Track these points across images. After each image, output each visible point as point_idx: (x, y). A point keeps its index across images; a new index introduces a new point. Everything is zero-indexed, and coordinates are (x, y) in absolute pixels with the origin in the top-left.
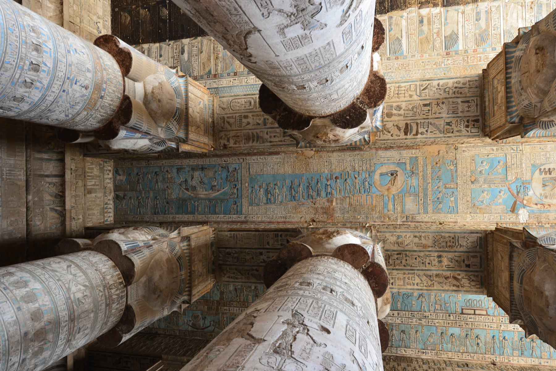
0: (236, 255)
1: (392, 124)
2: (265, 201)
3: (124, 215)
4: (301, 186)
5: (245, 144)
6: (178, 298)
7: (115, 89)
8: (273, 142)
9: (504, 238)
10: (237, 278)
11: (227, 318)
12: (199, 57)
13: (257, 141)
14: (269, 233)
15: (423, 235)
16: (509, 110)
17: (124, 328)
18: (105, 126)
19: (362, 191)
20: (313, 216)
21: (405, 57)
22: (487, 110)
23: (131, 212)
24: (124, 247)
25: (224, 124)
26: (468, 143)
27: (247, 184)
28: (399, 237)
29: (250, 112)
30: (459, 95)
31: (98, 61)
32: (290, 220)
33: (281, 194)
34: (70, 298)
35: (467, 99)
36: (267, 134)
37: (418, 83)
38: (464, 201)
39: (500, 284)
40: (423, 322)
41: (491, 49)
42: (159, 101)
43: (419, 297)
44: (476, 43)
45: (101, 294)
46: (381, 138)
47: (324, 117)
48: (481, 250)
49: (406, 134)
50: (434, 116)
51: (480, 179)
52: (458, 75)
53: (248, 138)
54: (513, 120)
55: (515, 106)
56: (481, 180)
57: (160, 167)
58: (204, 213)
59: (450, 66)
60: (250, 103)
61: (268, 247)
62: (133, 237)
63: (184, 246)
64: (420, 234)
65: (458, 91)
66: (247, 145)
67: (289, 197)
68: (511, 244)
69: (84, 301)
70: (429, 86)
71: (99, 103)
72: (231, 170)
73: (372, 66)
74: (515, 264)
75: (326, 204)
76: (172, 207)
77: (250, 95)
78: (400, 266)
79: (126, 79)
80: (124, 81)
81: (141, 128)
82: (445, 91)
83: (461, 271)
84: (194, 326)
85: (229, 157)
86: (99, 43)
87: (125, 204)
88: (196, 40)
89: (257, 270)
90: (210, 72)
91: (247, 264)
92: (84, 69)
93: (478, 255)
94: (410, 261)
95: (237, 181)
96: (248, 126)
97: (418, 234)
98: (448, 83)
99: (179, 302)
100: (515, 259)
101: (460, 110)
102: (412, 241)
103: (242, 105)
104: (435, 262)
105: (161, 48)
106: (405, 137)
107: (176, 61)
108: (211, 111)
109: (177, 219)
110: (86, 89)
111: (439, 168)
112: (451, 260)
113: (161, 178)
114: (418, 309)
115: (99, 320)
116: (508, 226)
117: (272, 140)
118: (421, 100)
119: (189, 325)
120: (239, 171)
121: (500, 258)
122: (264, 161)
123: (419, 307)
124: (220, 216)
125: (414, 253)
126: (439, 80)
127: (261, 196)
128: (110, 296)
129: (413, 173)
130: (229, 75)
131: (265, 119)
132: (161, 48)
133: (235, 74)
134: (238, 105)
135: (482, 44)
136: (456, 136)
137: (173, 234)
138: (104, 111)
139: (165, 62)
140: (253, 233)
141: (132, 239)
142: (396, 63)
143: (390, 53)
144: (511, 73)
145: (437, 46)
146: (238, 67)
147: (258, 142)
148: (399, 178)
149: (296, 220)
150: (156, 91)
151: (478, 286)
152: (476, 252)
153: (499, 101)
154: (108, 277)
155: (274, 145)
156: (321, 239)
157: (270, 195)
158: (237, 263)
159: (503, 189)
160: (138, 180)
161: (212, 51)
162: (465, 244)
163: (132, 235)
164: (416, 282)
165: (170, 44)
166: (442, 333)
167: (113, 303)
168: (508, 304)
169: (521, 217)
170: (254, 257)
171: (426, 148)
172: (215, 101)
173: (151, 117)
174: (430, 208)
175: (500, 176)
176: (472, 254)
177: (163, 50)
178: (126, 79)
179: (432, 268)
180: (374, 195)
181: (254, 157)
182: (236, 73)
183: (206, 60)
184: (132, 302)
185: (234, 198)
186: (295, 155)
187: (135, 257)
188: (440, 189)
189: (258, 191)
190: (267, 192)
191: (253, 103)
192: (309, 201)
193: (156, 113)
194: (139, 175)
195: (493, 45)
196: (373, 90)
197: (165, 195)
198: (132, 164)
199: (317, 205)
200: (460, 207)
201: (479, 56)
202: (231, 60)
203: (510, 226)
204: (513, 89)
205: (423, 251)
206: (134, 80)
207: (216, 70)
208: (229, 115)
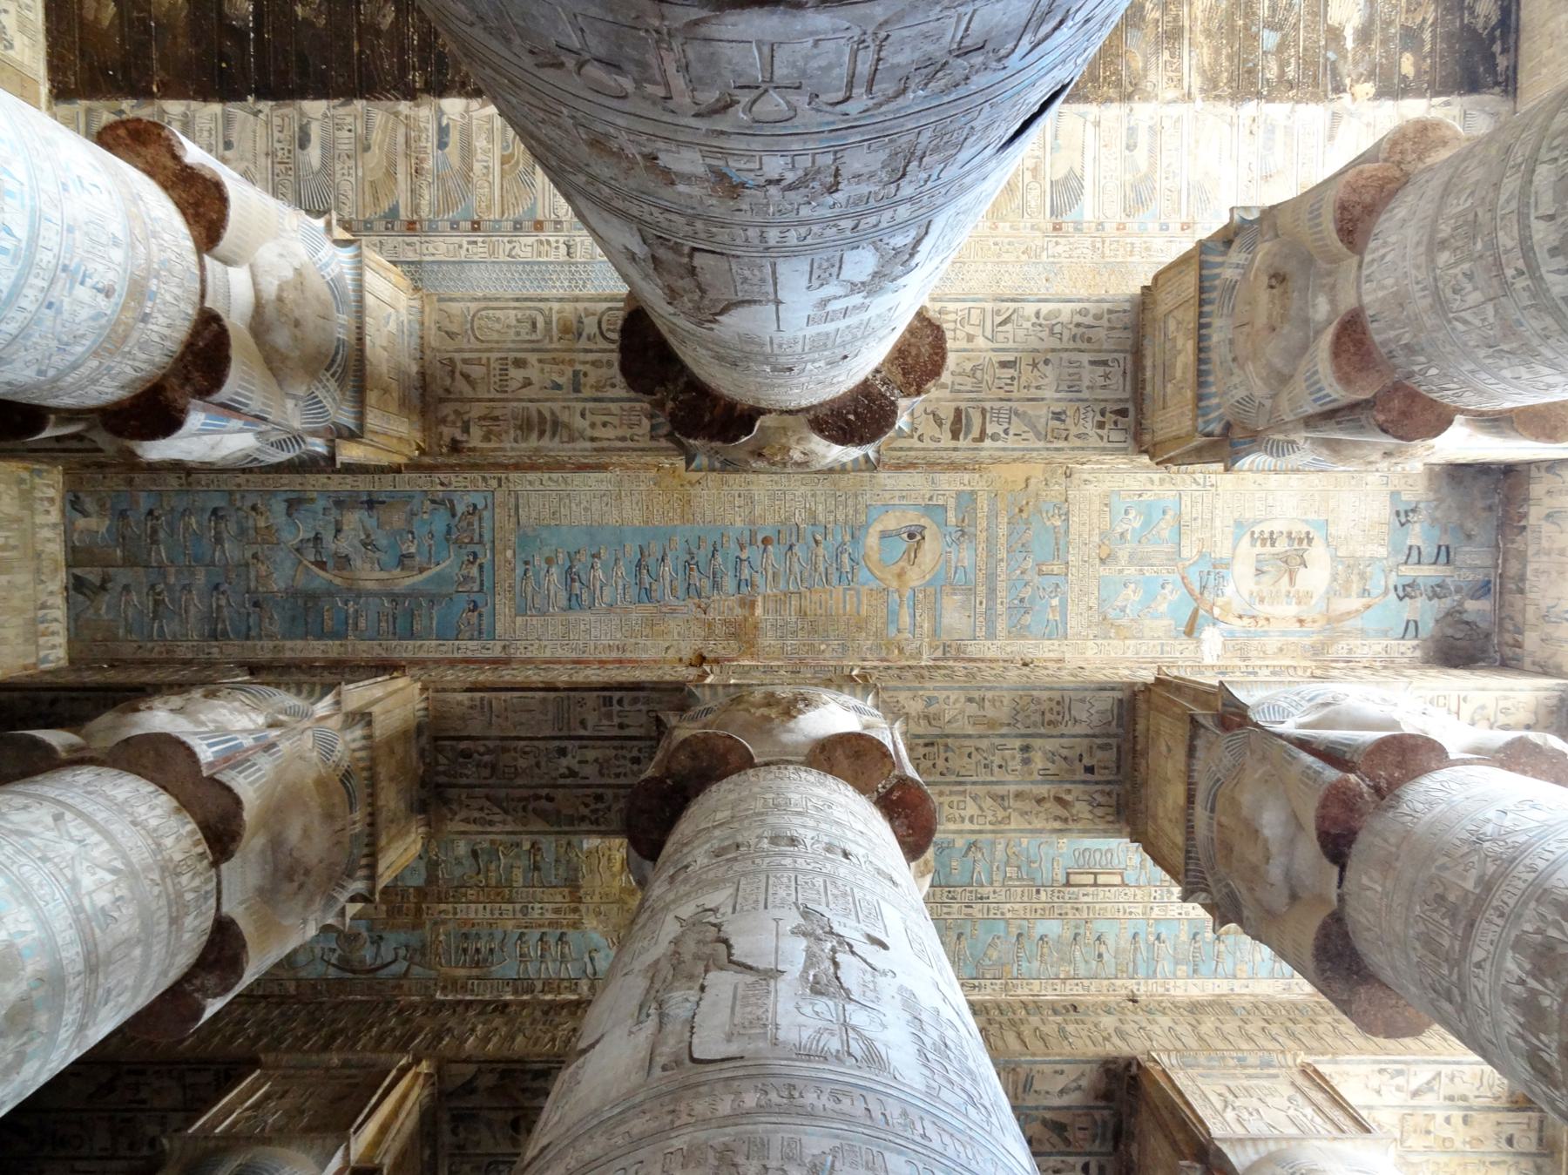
0: (486, 758)
2: (564, 603)
3: (105, 640)
4: (668, 560)
5: (516, 441)
6: (343, 887)
7: (178, 291)
8: (601, 439)
9: (1175, 703)
10: (491, 823)
11: (448, 934)
13: (554, 435)
14: (585, 694)
15: (989, 695)
16: (1203, 404)
17: (211, 981)
18: (137, 397)
19: (834, 578)
20: (699, 644)
22: (1149, 389)
23: (129, 631)
24: (206, 753)
25: (453, 379)
26: (1098, 462)
27: (509, 553)
28: (930, 701)
29: (533, 350)
30: (1085, 346)
31: (134, 210)
32: (634, 656)
33: (612, 581)
35: (1103, 357)
36: (583, 415)
37: (988, 306)
38: (1083, 607)
39: (1161, 813)
40: (976, 911)
41: (1157, 226)
42: (297, 324)
43: (969, 849)
45: (156, 890)
47: (790, 412)
48: (1121, 731)
49: (955, 436)
50: (1024, 393)
51: (1120, 554)
52: (1083, 293)
53: (527, 426)
54: (1209, 429)
55: (1215, 395)
56: (1123, 555)
57: (231, 493)
58: (377, 636)
60: (534, 325)
61: (582, 732)
62: (214, 721)
63: (354, 740)
64: (981, 693)
66: (524, 445)
67: (633, 591)
68: (1193, 721)
69: (116, 914)
70: (1014, 317)
71: (135, 335)
72: (460, 509)
74: (1198, 765)
75: (738, 611)
76: (271, 618)
77: (531, 300)
78: (930, 774)
79: (207, 259)
80: (202, 267)
81: (246, 405)
82: (1052, 333)
83: (1074, 782)
84: (344, 964)
85: (454, 472)
86: (111, 141)
87: (108, 607)
88: (348, 109)
89: (550, 799)
90: (394, 211)
91: (519, 781)
92: (104, 240)
93: (1113, 741)
94: (955, 763)
95: (481, 542)
96: (524, 390)
97: (976, 695)
98: (1059, 311)
99: (343, 898)
100: (1200, 754)
101: (1086, 383)
102: (962, 712)
104: (1016, 764)
105: (228, 121)
106: (953, 444)
107: (282, 167)
108: (415, 341)
109: (288, 654)
110: (107, 296)
111: (1027, 522)
112: (1051, 757)
113: (233, 528)
114: (967, 881)
115: (153, 963)
116: (1183, 674)
117: (596, 434)
119: (328, 963)
120: (486, 514)
121: (1164, 749)
122: (563, 487)
123: (968, 874)
125: (967, 742)
126: (1039, 301)
127: (552, 588)
128: (180, 895)
129: (963, 533)
130: (454, 226)
131: (576, 374)
132: (228, 121)
133: (476, 226)
134: (497, 326)
136: (1073, 449)
137: (320, 705)
138: (144, 357)
139: (243, 165)
140: (541, 694)
141: (212, 726)
144: (1209, 314)
147: (557, 439)
148: (927, 545)
149: (651, 654)
150: (290, 296)
151: (1110, 818)
152: (1108, 736)
153: (1179, 374)
154: (169, 842)
155: (603, 449)
156: (768, 719)
157: (577, 584)
158: (490, 781)
159: (1171, 577)
160: (154, 531)
161: (401, 147)
162: (1084, 716)
163: (211, 716)
164: (967, 813)
166: (1020, 935)
167: (187, 914)
168: (1178, 858)
169: (1205, 647)
170: (543, 764)
171: (996, 471)
172: (427, 309)
173: (271, 369)
174: (1001, 625)
175: (1166, 548)
176: (1099, 741)
177: (237, 126)
178: (207, 259)
179: (1009, 778)
180: (864, 590)
181: (531, 476)
182: (478, 223)
183: (380, 174)
184: (231, 908)
186: (654, 472)
187: (240, 778)
188: (1027, 577)
189: (543, 573)
190: (570, 576)
192: (689, 602)
193: (287, 358)
194: (157, 518)
196: (914, 352)
197: (248, 579)
198: (130, 482)
199: (710, 617)
200: (1072, 622)
201: (1129, 240)
202: (461, 182)
203: (1188, 675)
204: (1214, 356)
205: (987, 736)
206: (226, 262)
207: (416, 209)
208: (467, 355)
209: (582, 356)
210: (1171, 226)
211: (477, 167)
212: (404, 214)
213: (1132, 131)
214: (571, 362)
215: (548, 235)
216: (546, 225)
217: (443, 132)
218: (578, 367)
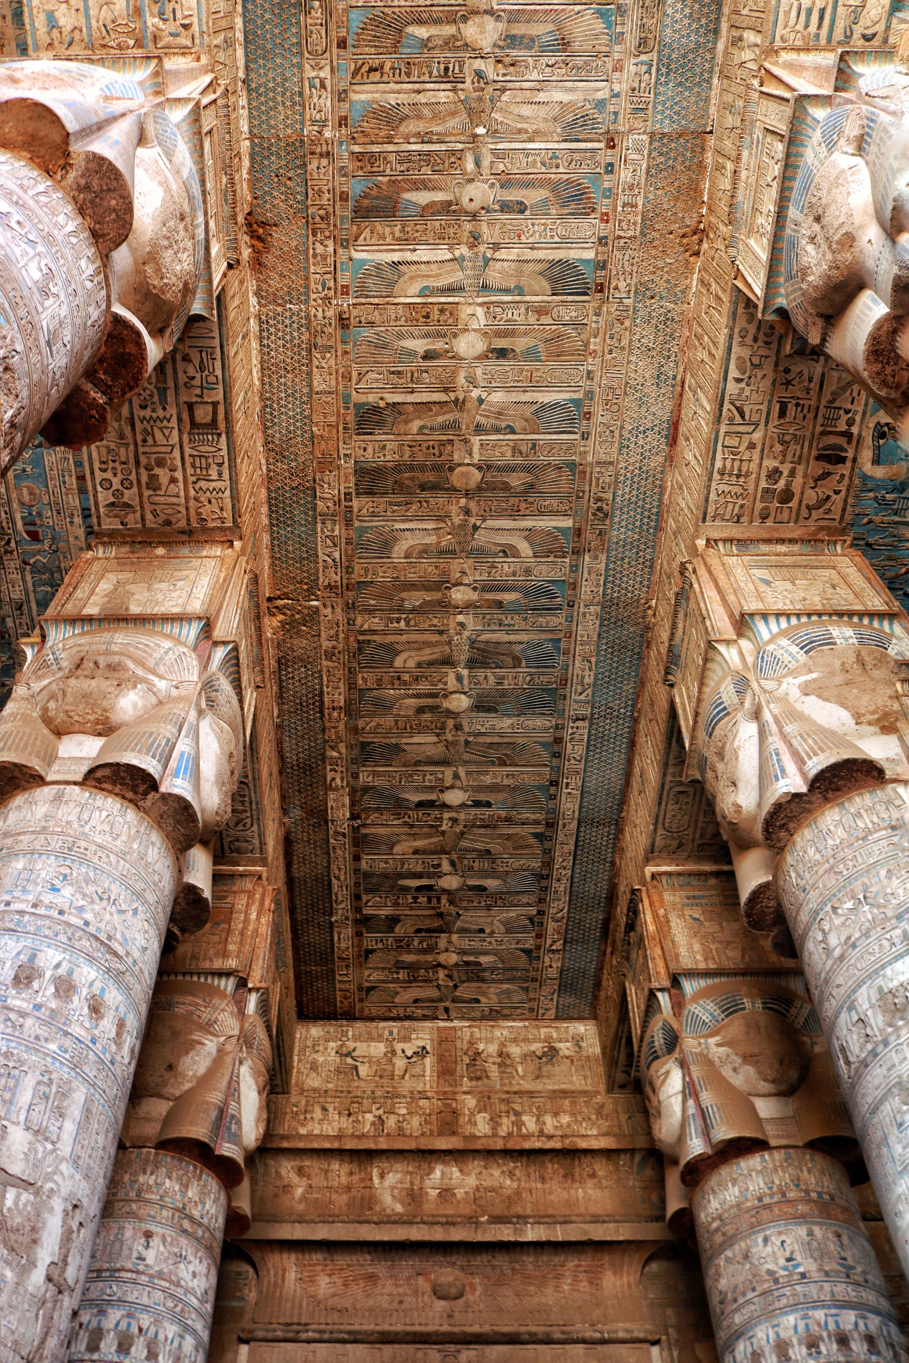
1: (810, 491)
21: (590, 394)
41: (606, 177)
44: (585, 214)
59: (633, 283)
60: (681, 792)
65: (766, 335)
70: (738, 404)
90: (537, 836)
98: (739, 358)
118: (767, 423)
126: (725, 379)
130: (552, 797)
133: (554, 783)
134: (679, 817)
135: (590, 198)
142: (600, 416)
143: (570, 432)
145: (574, 314)
177: (467, 926)
191: (682, 789)
195: (598, 170)
201: (620, 209)
207: (537, 822)
208: (698, 835)
210: (609, 160)
211: (506, 782)
212: (540, 829)
213: (505, 207)
215: (567, 735)
216: (557, 735)
217: (477, 804)
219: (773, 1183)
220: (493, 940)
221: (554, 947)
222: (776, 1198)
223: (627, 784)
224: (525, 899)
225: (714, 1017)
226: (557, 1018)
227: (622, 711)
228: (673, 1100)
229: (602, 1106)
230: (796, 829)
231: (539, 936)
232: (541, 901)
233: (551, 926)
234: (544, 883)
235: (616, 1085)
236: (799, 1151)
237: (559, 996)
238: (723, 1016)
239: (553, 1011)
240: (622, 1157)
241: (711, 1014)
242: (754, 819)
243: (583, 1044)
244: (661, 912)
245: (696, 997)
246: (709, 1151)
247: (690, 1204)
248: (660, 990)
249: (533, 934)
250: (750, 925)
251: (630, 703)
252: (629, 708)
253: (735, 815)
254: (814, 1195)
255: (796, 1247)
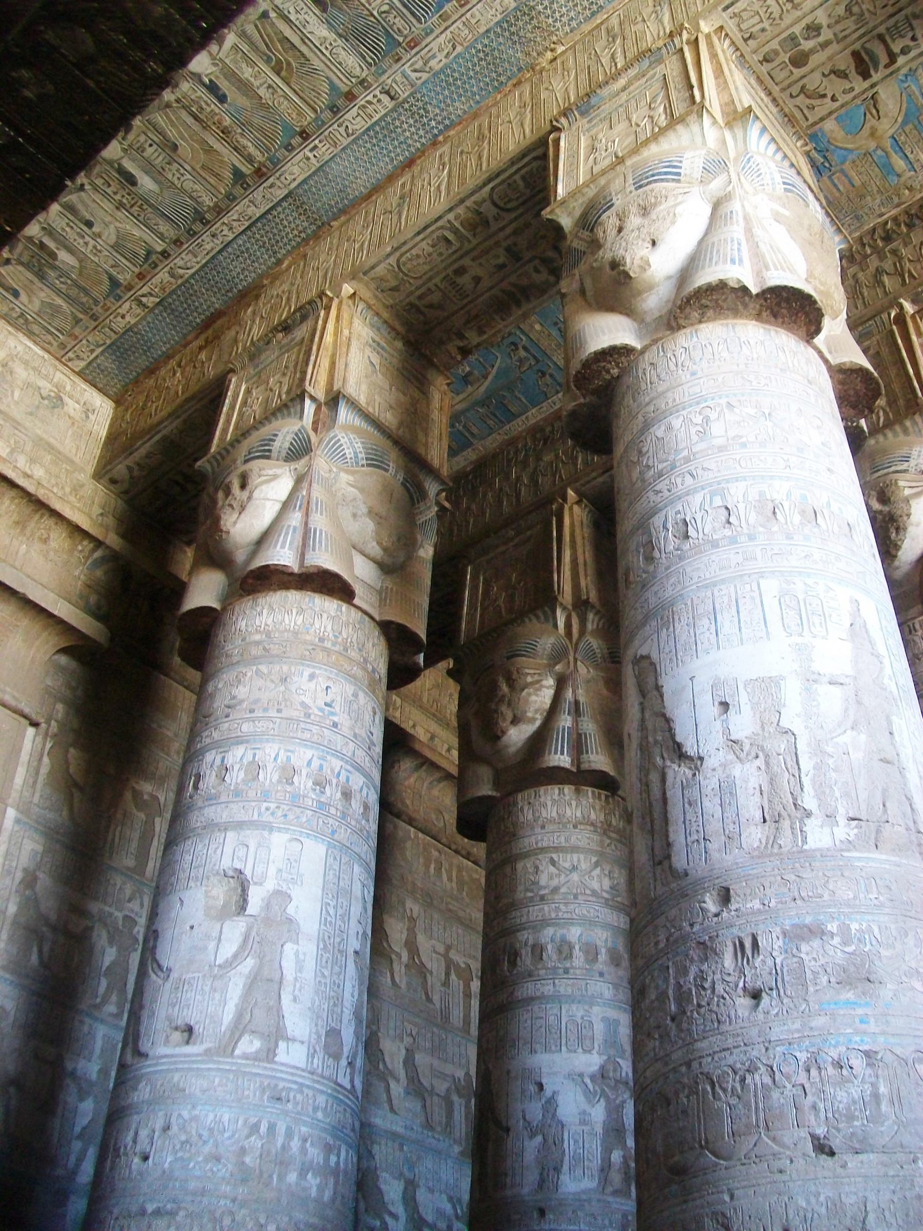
12: (181, 161)
27: (538, 327)
29: (462, 257)
34: (607, 899)
46: (811, 121)
58: (491, 431)
73: (826, 361)
90: (238, 175)
103: (430, 255)
107: (136, 208)
124: (529, 413)
130: (289, 148)
131: (508, 250)
133: (304, 135)
134: (421, 261)
146: (294, 116)
154: (593, 816)
161: (196, 126)
165: (82, 185)
177: (80, 206)
185: (530, 367)
191: (450, 236)
207: (250, 159)
209: (501, 235)
211: (262, 92)
212: (246, 169)
214: (497, 244)
216: (355, 91)
217: (212, 88)
218: (504, 244)
219: (340, 633)
220: (92, 242)
221: (144, 300)
222: (337, 648)
223: (367, 197)
224: (164, 227)
225: (356, 457)
226: (80, 374)
227: (433, 123)
228: (268, 504)
229: (82, 486)
230: (709, 320)
231: (141, 276)
232: (177, 242)
233: (163, 276)
234: (197, 227)
235: (107, 477)
236: (373, 624)
237: (102, 353)
238: (364, 462)
239: (82, 364)
240: (85, 543)
241: (355, 453)
242: (650, 287)
243: (92, 417)
244: (346, 332)
245: (347, 428)
246: (296, 569)
247: (224, 609)
248: (313, 398)
249: (137, 270)
250: (576, 375)
251: (447, 122)
252: (441, 127)
253: (637, 270)
254: (370, 668)
255: (339, 699)
